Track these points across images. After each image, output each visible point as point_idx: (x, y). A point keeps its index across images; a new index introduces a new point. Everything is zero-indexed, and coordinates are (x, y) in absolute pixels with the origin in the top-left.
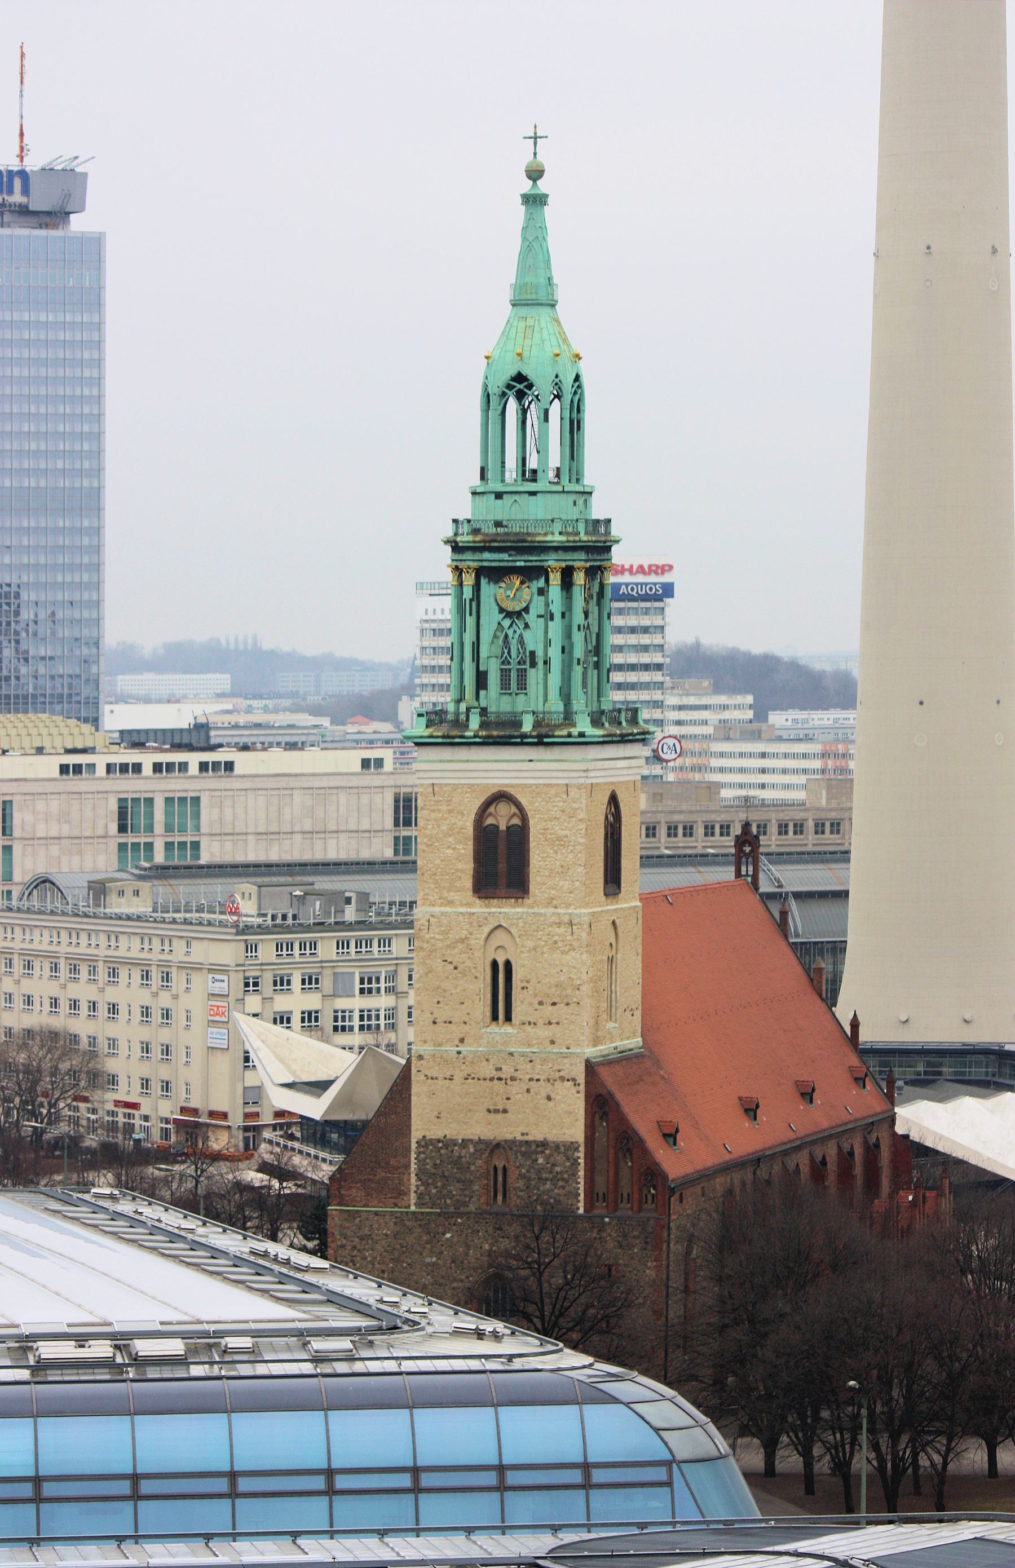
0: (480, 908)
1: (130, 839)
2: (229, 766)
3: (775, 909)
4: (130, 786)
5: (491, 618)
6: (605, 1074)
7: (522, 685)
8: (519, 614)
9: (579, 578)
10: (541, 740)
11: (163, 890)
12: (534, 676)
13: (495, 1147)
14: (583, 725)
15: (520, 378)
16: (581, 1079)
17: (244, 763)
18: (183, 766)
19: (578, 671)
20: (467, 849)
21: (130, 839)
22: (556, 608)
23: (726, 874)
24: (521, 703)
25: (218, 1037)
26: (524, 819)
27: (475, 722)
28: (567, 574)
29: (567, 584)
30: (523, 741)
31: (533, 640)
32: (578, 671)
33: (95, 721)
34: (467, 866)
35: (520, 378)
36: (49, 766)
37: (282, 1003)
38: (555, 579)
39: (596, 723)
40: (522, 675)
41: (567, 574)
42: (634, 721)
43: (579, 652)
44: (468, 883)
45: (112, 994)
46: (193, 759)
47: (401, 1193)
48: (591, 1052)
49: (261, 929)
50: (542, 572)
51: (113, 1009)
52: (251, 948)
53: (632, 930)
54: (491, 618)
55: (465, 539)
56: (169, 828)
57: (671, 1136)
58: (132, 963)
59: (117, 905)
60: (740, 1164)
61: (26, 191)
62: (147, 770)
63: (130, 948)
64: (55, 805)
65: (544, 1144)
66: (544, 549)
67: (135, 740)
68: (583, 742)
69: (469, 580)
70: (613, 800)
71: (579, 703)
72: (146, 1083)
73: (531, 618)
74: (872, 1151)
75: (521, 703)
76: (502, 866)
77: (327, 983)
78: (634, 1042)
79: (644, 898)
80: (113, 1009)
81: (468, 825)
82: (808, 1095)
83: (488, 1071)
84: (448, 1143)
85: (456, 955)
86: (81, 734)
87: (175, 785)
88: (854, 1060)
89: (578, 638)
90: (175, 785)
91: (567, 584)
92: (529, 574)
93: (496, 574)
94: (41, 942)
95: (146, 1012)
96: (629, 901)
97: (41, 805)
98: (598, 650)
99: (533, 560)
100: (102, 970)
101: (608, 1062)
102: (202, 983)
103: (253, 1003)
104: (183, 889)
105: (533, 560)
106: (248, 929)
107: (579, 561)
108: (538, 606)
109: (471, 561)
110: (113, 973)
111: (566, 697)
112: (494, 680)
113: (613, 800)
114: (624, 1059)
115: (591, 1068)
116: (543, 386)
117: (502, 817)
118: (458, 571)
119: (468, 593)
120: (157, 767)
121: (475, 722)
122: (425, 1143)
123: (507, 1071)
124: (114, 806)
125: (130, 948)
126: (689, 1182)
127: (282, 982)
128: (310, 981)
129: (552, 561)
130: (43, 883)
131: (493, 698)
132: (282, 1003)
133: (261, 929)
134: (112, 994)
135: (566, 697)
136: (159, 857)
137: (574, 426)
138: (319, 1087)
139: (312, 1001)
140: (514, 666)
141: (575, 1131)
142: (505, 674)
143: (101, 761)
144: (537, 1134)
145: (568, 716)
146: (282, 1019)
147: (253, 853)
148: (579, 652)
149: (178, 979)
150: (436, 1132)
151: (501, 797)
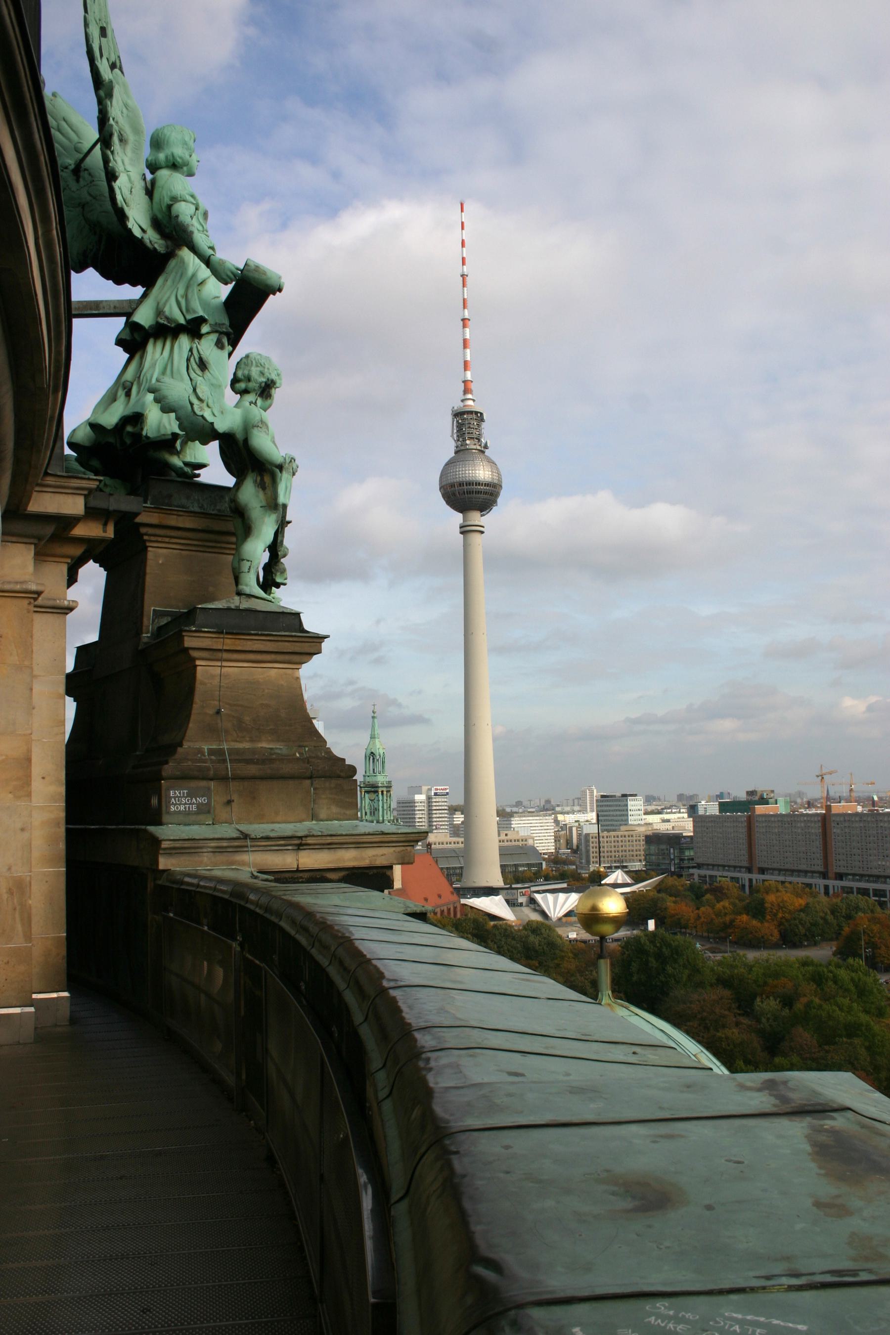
5: (367, 801)
9: (385, 793)
12: (376, 813)
19: (385, 811)
28: (382, 792)
38: (380, 793)
40: (374, 812)
41: (382, 792)
43: (385, 808)
71: (385, 818)
89: (385, 805)
93: (368, 792)
99: (376, 789)
105: (376, 789)
107: (385, 789)
119: (363, 796)
140: (372, 811)
142: (371, 812)
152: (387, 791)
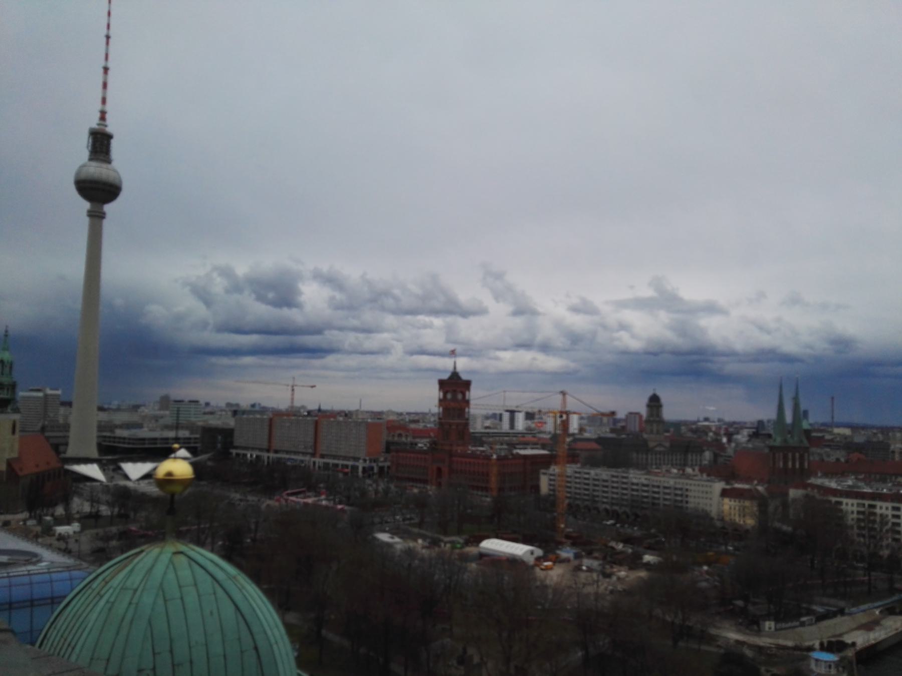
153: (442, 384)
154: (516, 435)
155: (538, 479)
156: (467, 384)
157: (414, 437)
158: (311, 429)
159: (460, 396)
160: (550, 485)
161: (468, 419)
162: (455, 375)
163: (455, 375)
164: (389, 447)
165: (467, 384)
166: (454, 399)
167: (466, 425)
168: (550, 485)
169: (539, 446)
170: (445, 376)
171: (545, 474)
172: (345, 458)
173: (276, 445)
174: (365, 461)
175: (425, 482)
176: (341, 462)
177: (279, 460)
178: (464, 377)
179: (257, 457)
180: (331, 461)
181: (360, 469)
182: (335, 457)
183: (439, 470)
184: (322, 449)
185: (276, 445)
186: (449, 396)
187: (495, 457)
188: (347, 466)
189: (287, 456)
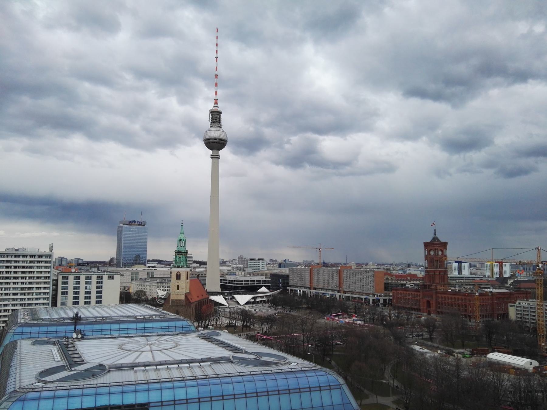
0: (176, 281)
1: (148, 275)
2: (157, 269)
3: (200, 281)
4: (148, 271)
5: (178, 258)
6: (186, 294)
7: (180, 263)
8: (180, 258)
9: (185, 255)
10: (182, 267)
11: (151, 279)
12: (181, 262)
13: (177, 300)
14: (185, 266)
15: (181, 239)
16: (184, 294)
17: (158, 269)
18: (153, 269)
19: (185, 262)
20: (176, 276)
21: (148, 275)
22: (183, 257)
23: (196, 278)
24: (180, 265)
25: (155, 291)
26: (180, 273)
27: (176, 266)
28: (184, 254)
29: (184, 255)
30: (180, 268)
31: (181, 260)
32: (185, 262)
33: (146, 266)
34: (175, 278)
35: (181, 239)
36: (142, 269)
37: (160, 288)
38: (183, 255)
39: (186, 266)
41: (184, 254)
42: (189, 266)
43: (185, 261)
44: (176, 279)
45: (146, 288)
46: (154, 269)
47: (169, 304)
48: (185, 292)
49: (159, 282)
50: (182, 254)
51: (146, 289)
52: (158, 284)
53: (189, 283)
54: (178, 258)
55: (176, 252)
56: (152, 274)
57: (192, 299)
58: (148, 285)
59: (147, 281)
60: (197, 301)
61: (141, 223)
62: (150, 270)
63: (148, 284)
64: (142, 272)
65: (181, 300)
66: (182, 252)
67: (149, 267)
68: (185, 268)
69: (176, 255)
70: (187, 272)
71: (185, 265)
72: (149, 295)
73: (181, 258)
74: (208, 300)
75: (180, 265)
76: (178, 278)
77: (164, 287)
78: (189, 291)
79: (190, 280)
80: (146, 289)
81: (176, 274)
82: (203, 296)
83: (177, 294)
84: (173, 300)
85: (175, 285)
86: (144, 266)
87: (152, 271)
88: (206, 293)
89: (185, 259)
90: (152, 271)
91: (184, 255)
92: (181, 254)
93: (179, 254)
94: (140, 283)
95: (149, 289)
96: (189, 280)
97: (141, 272)
98: (186, 260)
99: (182, 253)
100: (146, 286)
101: (186, 293)
102: (154, 287)
103: (158, 288)
104: (152, 279)
105: (182, 253)
106: (158, 282)
107: (185, 253)
108: (182, 257)
109: (176, 253)
110: (146, 286)
111: (184, 264)
112: (178, 263)
113: (187, 272)
114: (188, 293)
115: (185, 293)
116: (183, 240)
117: (178, 274)
118: (175, 254)
120: (151, 269)
121: (176, 266)
122: (171, 300)
123: (178, 294)
124: (147, 272)
125: (148, 284)
126: (193, 303)
127: (161, 287)
128: (163, 287)
129: (183, 253)
130: (141, 279)
131: (178, 264)
132: (160, 288)
133: (159, 282)
134: (146, 288)
135: (184, 264)
136: (151, 277)
137: (185, 243)
138: (163, 295)
139: (163, 288)
141: (184, 299)
142: (179, 262)
143: (146, 269)
144: (181, 299)
145: (184, 266)
146: (160, 290)
147: (159, 276)
148: (185, 261)
149: (152, 286)
150: (172, 299)
151: (178, 272)
152: (186, 254)
153: (426, 245)
154: (462, 278)
155: (507, 309)
156: (445, 244)
157: (397, 280)
158: (336, 275)
159: (440, 253)
160: (517, 314)
161: (446, 268)
162: (435, 239)
163: (435, 239)
164: (388, 287)
165: (445, 244)
166: (436, 254)
167: (446, 272)
168: (517, 314)
169: (489, 286)
170: (429, 240)
171: (511, 306)
172: (360, 293)
173: (315, 285)
174: (374, 295)
175: (419, 310)
176: (357, 296)
177: (317, 295)
178: (442, 239)
179: (303, 292)
180: (351, 295)
181: (371, 301)
182: (353, 293)
183: (428, 302)
184: (345, 287)
185: (315, 285)
186: (432, 253)
187: (477, 294)
188: (362, 299)
189: (322, 292)
